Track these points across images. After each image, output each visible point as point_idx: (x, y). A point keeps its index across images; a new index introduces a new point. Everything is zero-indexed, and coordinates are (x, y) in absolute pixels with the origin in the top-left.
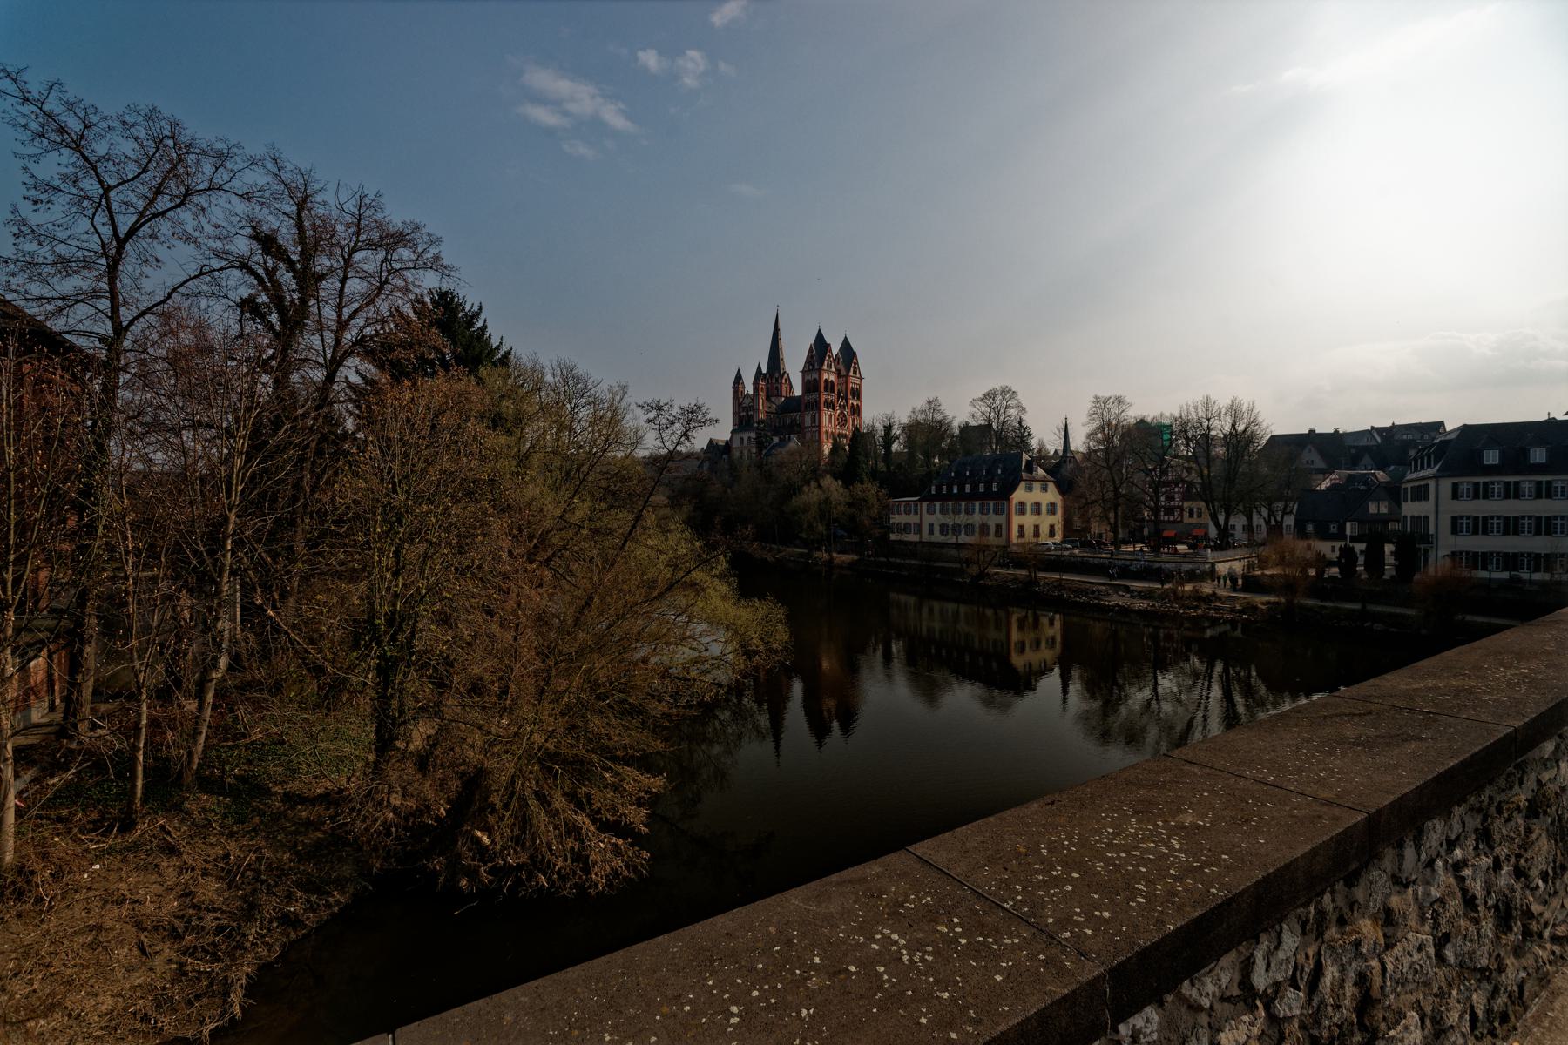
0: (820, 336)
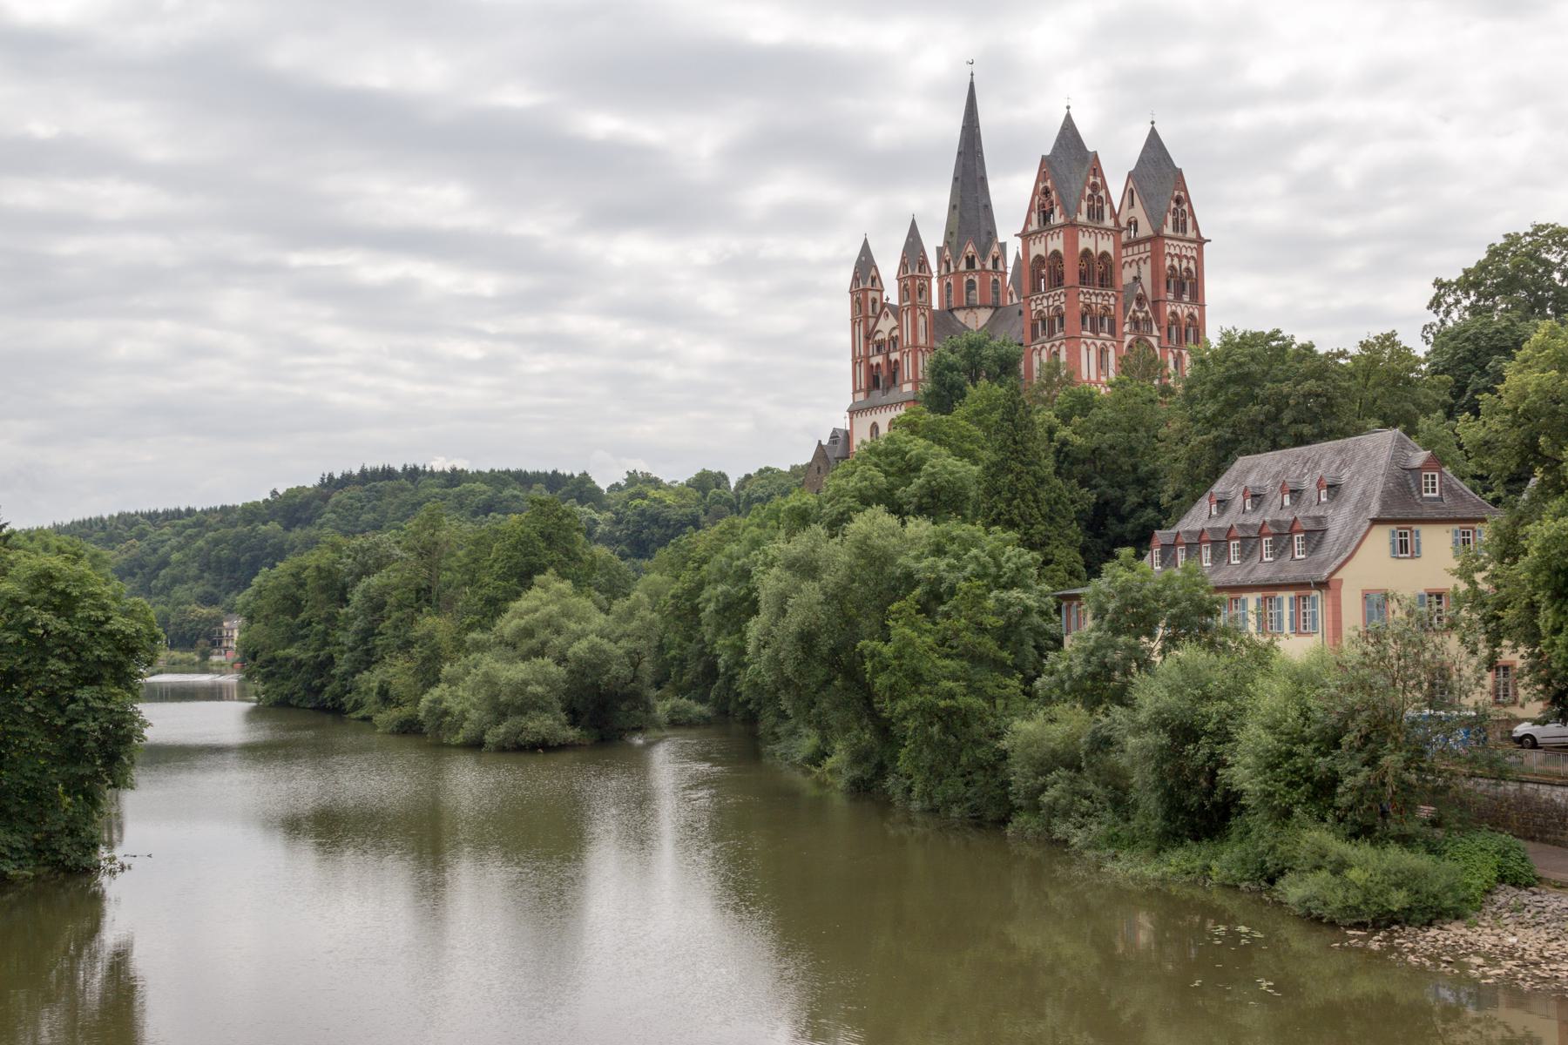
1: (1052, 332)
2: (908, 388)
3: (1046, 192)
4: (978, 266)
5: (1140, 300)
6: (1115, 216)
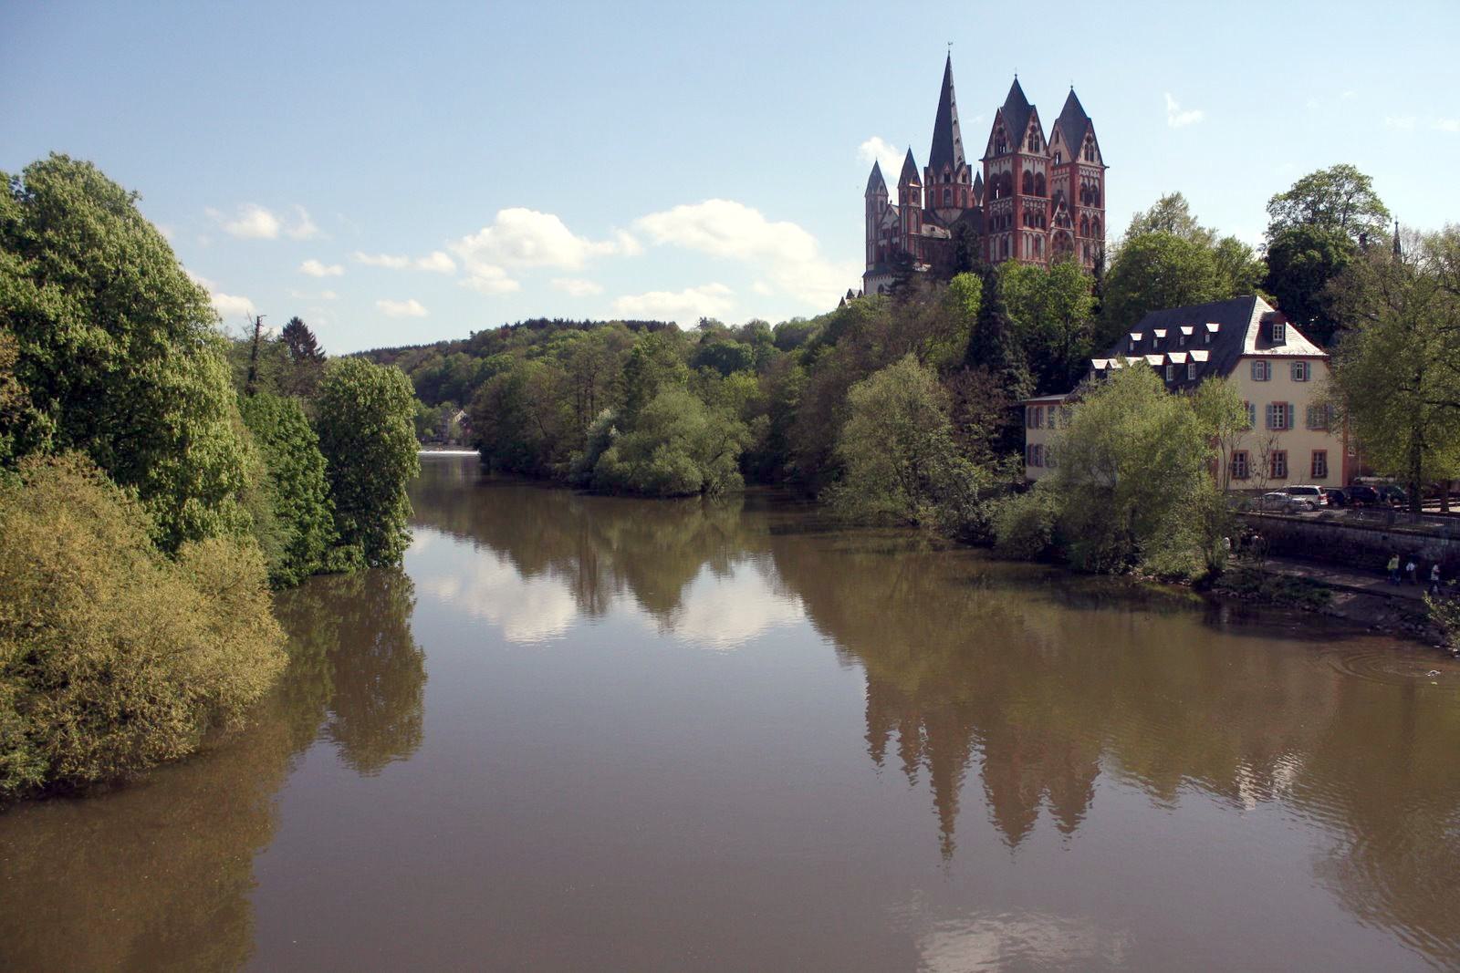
0: (1016, 93)
3: (1001, 132)
4: (952, 180)
5: (1062, 208)
6: (1046, 147)
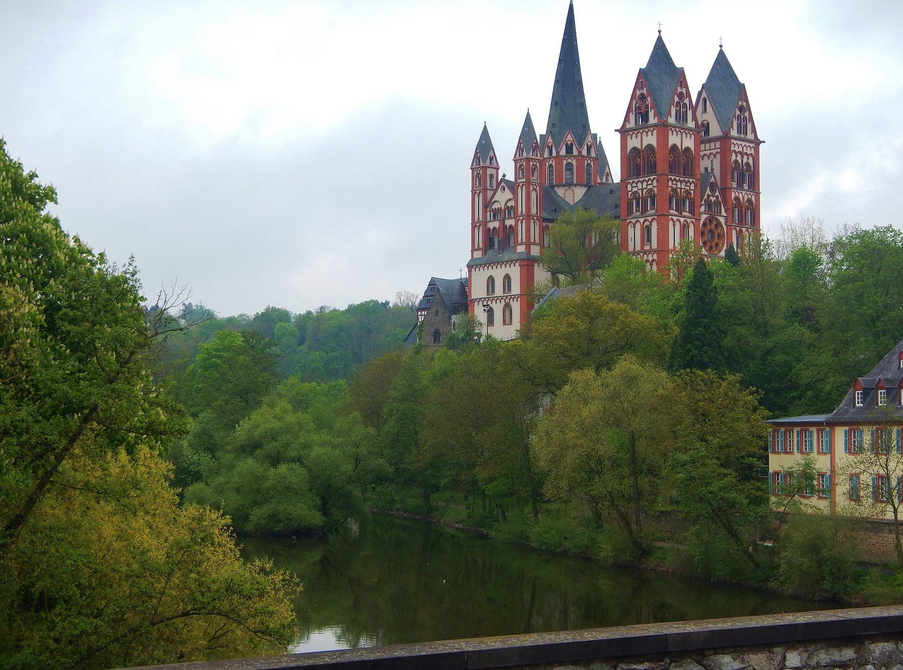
0: (660, 52)
1: (645, 210)
2: (521, 249)
4: (575, 152)
5: (713, 187)
